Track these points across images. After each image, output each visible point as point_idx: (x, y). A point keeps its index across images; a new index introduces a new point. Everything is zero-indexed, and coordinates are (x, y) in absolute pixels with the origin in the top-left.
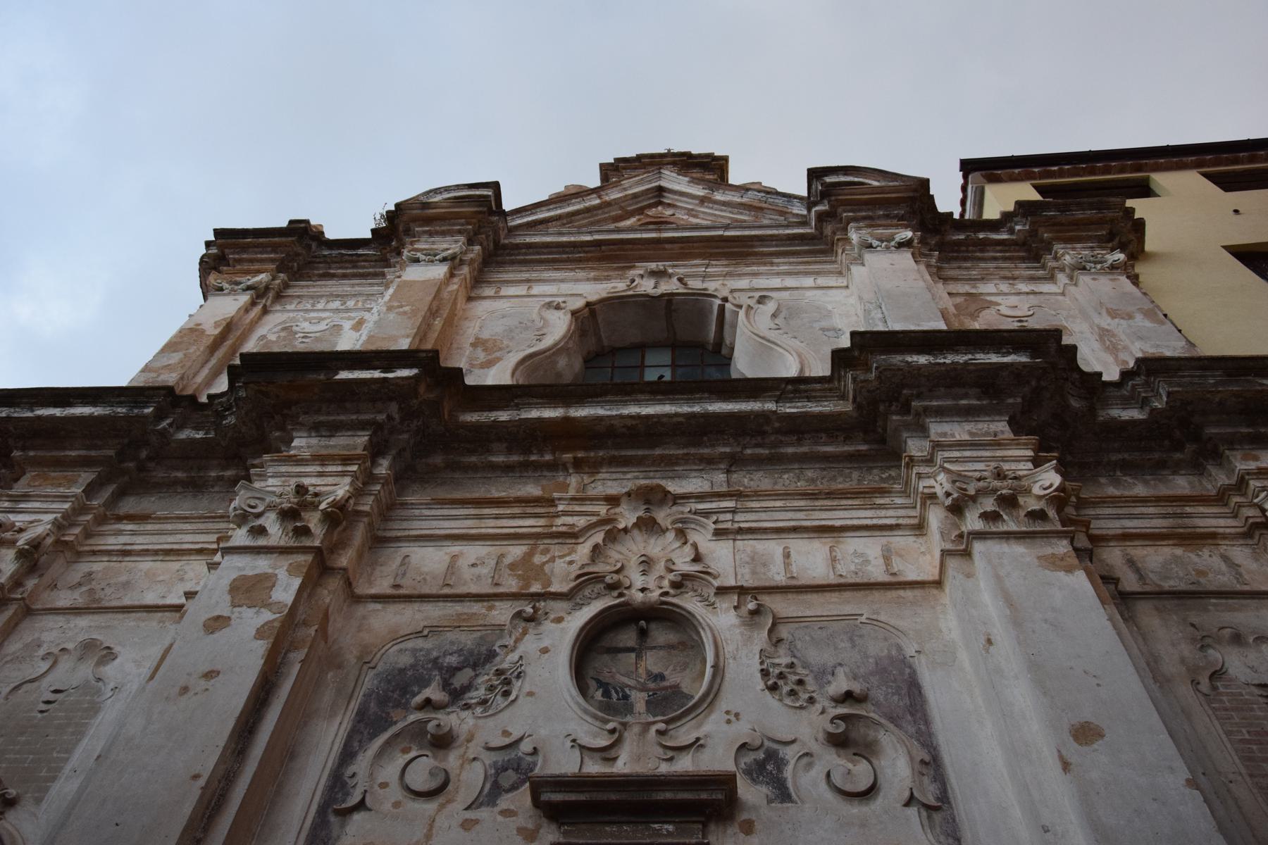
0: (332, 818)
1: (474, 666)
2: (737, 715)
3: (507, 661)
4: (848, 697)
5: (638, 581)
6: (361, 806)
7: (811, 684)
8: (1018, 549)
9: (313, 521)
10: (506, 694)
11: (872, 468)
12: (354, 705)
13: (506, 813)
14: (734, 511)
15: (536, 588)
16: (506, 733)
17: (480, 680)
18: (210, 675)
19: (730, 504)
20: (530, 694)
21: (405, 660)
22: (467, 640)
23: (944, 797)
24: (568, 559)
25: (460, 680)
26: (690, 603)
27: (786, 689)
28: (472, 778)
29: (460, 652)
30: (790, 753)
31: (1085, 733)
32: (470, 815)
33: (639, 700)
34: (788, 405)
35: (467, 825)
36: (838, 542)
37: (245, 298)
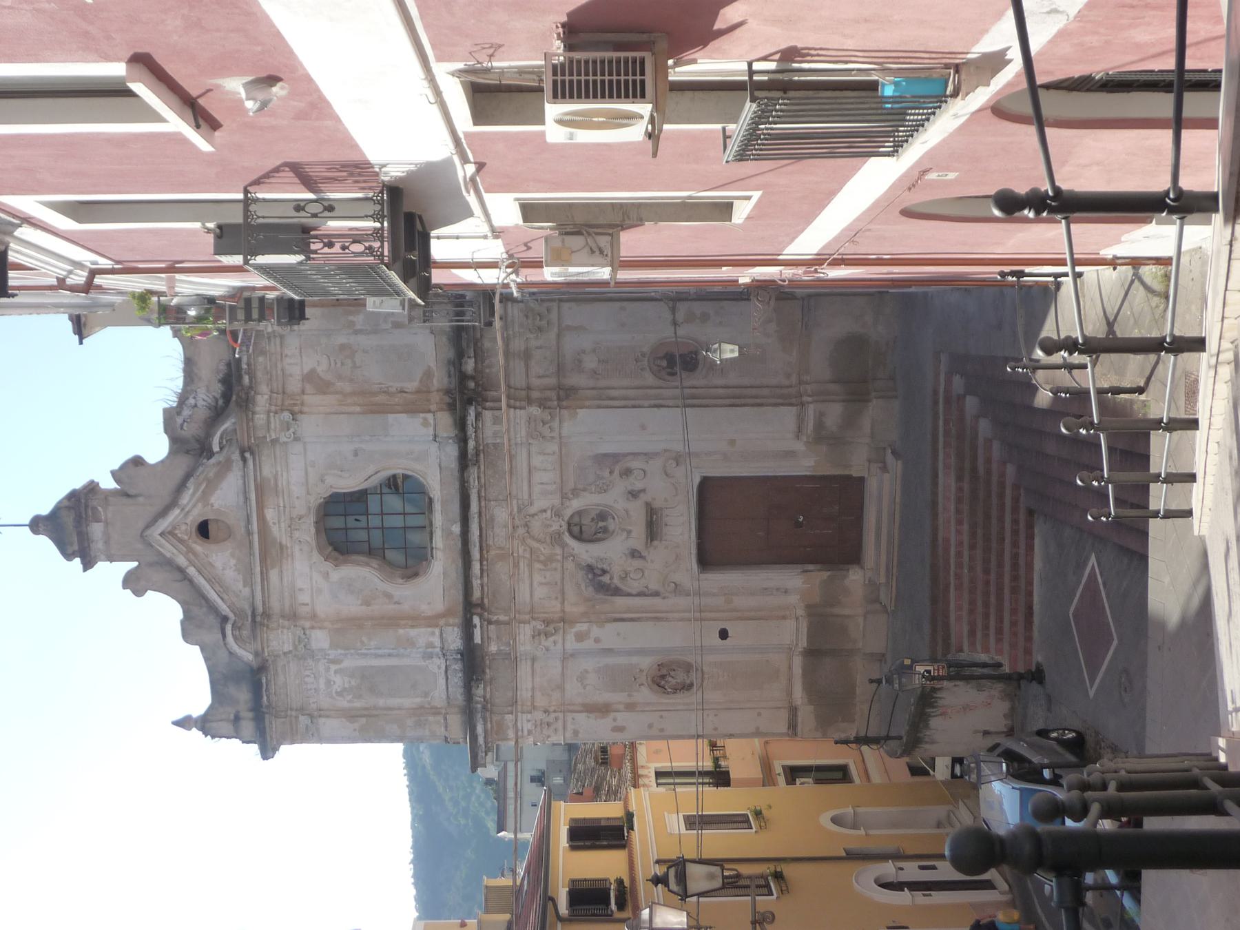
0: (650, 593)
1: (593, 569)
2: (616, 500)
3: (590, 561)
4: (611, 473)
5: (555, 527)
6: (647, 587)
7: (604, 481)
8: (565, 425)
9: (551, 628)
10: (606, 559)
11: (488, 451)
12: (610, 598)
13: (649, 552)
14: (518, 499)
15: (559, 558)
16: (621, 557)
17: (599, 566)
18: (618, 634)
19: (515, 502)
20: (606, 553)
21: (591, 589)
22: (581, 574)
23: (645, 454)
24: (543, 549)
25: (599, 572)
26: (568, 513)
27: (605, 487)
28: (637, 563)
29: (587, 575)
30: (630, 488)
31: (643, 427)
32: (649, 561)
33: (601, 524)
34: (472, 483)
35: (652, 561)
36: (535, 468)
37: (322, 720)
